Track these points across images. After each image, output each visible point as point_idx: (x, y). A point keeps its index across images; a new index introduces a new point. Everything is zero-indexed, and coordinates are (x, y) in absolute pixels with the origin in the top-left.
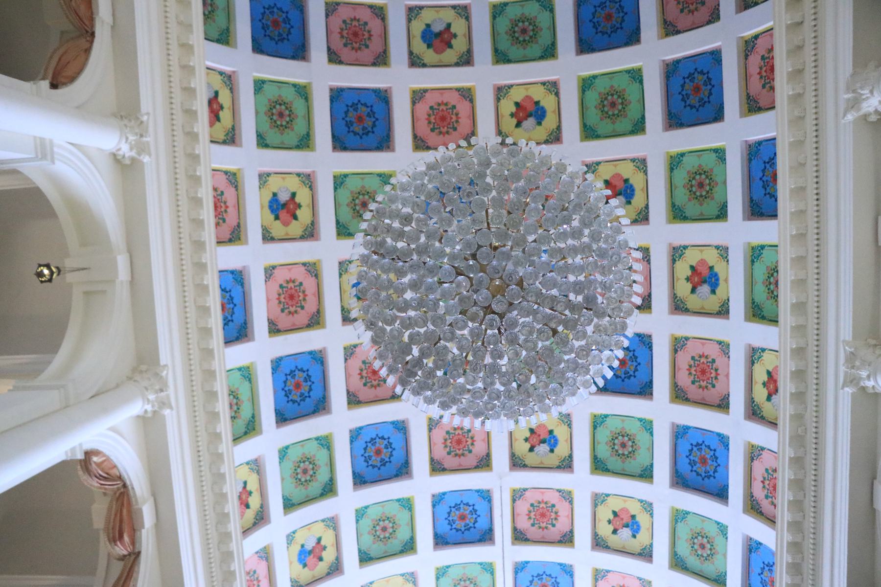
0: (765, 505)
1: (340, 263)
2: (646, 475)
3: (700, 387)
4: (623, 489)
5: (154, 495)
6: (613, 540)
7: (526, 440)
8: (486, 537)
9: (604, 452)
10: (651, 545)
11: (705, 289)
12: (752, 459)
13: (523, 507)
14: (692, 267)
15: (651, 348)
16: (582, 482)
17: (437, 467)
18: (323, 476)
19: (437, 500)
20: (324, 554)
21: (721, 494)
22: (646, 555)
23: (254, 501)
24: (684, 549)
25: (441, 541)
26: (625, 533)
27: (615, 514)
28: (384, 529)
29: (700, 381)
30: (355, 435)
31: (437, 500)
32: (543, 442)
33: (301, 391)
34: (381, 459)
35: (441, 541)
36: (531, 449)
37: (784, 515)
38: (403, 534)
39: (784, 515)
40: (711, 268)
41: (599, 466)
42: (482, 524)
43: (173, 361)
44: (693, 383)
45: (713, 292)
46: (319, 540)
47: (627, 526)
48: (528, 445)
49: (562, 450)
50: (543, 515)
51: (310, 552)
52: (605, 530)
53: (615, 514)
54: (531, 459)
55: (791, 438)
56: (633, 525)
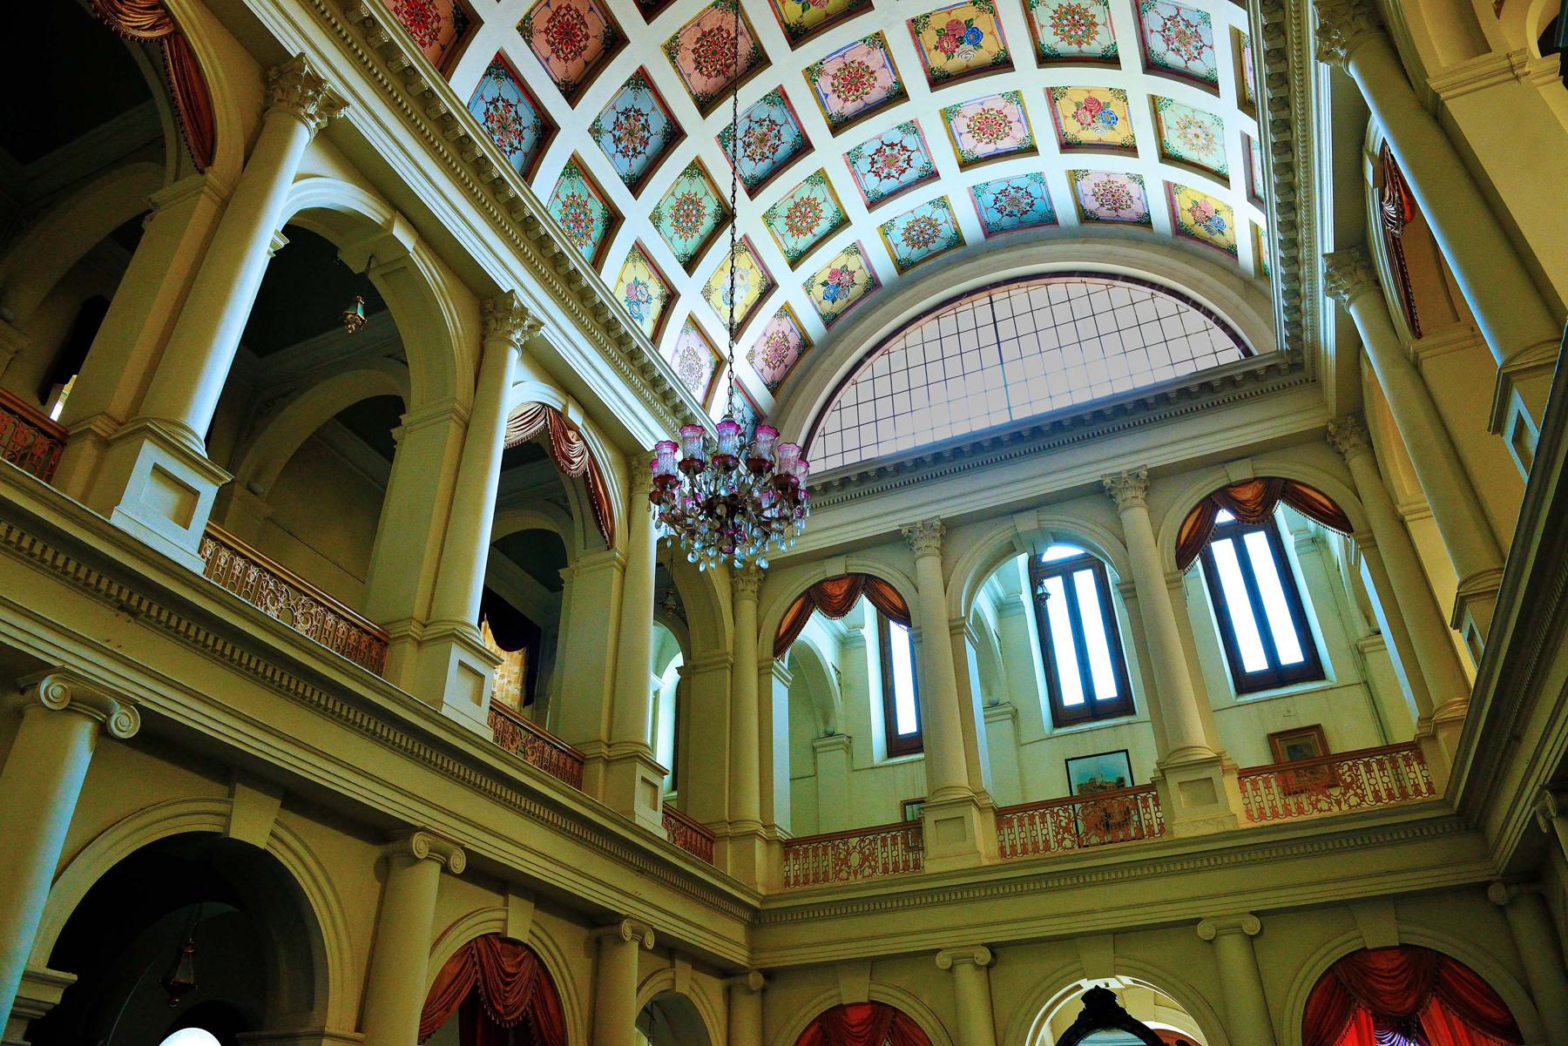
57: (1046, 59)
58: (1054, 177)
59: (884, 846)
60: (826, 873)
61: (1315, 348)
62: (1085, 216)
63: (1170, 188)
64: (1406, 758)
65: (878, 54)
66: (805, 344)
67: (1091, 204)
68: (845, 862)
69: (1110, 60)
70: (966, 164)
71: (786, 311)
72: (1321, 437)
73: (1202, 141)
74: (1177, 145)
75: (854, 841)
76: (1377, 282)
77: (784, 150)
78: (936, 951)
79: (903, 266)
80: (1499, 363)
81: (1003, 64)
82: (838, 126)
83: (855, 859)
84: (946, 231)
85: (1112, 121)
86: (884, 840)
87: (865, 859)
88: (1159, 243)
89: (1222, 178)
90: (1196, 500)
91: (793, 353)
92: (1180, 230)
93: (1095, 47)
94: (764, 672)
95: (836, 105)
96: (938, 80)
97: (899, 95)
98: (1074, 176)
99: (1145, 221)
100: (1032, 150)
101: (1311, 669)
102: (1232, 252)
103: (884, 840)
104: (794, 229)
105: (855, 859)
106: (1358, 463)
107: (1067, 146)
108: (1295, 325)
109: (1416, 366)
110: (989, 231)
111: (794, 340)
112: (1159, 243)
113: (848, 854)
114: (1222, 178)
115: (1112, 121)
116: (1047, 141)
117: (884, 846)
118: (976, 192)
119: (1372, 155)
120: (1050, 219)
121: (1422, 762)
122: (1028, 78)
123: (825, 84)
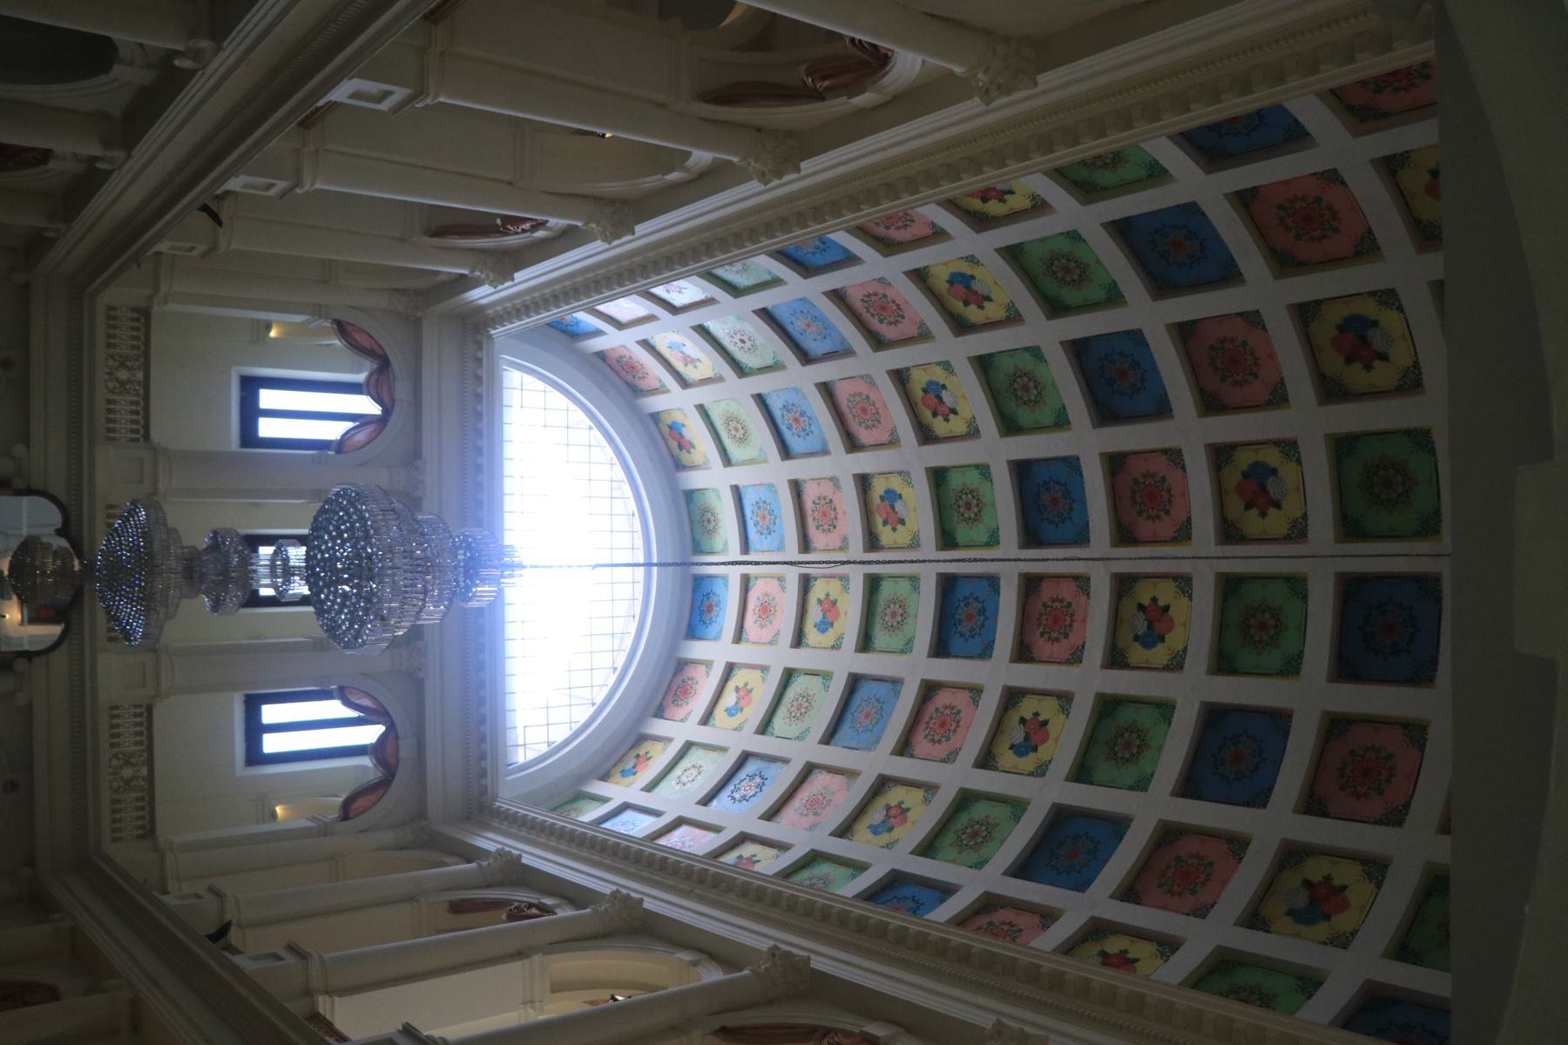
0: (983, 920)
1: (1393, 290)
2: (1081, 773)
3: (1168, 867)
4: (1066, 737)
5: (895, 98)
6: (1014, 717)
7: (1154, 600)
8: (1031, 537)
9: (1126, 715)
10: (996, 769)
11: (1302, 901)
12: (1043, 916)
13: (1067, 591)
14: (1344, 888)
15: (1247, 804)
16: (1089, 680)
17: (1115, 463)
18: (1070, 296)
19: (1072, 464)
20: (973, 307)
21: (1023, 869)
22: (986, 760)
23: (994, 207)
24: (979, 810)
25: (1022, 470)
26: (1018, 735)
27: (1045, 723)
28: (1026, 389)
29: (1177, 868)
30: (1136, 337)
31: (1072, 464)
32: (1150, 626)
33: (1172, 251)
34: (1114, 377)
35: (1022, 470)
36: (1141, 607)
37: (876, 913)
38: (1024, 416)
39: (958, 937)
40: (1328, 917)
41: (1107, 705)
42: (1145, 528)
43: (1044, 92)
44: (1178, 858)
45: (1290, 913)
46: (989, 299)
47: (1026, 739)
48: (1146, 602)
49: (1137, 653)
50: (1055, 621)
51: (968, 288)
52: (1027, 707)
53: (1045, 723)
54: (1129, 606)
55: (994, 954)
56: (1026, 747)
57: (789, 675)
59: (132, 403)
60: (114, 346)
62: (682, 665)
63: (668, 740)
64: (142, 827)
67: (690, 671)
68: (122, 365)
72: (421, 814)
73: (684, 779)
74: (695, 756)
75: (140, 376)
76: (489, 886)
78: (28, 444)
79: (689, 495)
80: (326, 956)
81: (798, 640)
83: (123, 375)
86: (137, 403)
87: (122, 384)
88: (640, 719)
89: (650, 788)
90: (389, 708)
91: (629, 378)
92: (642, 738)
93: (779, 722)
94: (318, 311)
98: (708, 664)
99: (660, 713)
100: (739, 636)
101: (255, 756)
102: (605, 777)
103: (137, 403)
104: (729, 419)
105: (123, 375)
106: (388, 837)
107: (730, 668)
109: (411, 899)
111: (643, 384)
112: (640, 719)
113: (130, 369)
114: (650, 788)
116: (739, 654)
117: (132, 403)
119: (558, 906)
121: (140, 837)
122: (783, 656)
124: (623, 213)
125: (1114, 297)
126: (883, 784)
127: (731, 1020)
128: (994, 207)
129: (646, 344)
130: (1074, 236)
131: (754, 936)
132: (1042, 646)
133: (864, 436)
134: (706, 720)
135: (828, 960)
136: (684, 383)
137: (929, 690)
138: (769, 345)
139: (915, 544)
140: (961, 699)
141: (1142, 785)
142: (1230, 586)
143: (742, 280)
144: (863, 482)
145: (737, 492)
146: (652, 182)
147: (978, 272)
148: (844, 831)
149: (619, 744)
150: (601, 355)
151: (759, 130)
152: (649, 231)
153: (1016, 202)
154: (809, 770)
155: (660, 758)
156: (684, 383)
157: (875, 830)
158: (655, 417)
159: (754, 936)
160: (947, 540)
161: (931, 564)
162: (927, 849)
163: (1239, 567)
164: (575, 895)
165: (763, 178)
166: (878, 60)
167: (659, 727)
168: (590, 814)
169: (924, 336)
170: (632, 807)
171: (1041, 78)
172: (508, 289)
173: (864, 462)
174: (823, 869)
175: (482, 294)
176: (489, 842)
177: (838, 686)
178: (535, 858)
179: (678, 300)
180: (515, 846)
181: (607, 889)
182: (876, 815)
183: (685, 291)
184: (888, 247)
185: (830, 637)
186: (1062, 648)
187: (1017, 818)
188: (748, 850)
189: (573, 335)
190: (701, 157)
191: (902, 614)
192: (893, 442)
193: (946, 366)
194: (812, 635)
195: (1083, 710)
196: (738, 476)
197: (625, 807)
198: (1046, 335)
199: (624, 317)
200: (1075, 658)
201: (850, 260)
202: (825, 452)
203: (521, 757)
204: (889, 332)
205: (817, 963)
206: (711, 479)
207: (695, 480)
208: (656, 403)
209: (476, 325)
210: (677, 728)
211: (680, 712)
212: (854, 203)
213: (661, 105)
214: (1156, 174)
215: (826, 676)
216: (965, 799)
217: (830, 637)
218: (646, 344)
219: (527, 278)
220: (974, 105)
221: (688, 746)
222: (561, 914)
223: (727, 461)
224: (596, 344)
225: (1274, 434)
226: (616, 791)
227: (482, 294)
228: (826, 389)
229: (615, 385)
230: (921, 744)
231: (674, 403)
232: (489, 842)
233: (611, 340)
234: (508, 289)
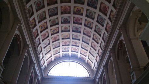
0: (108, 30)
8: (69, 23)
9: (88, 14)
24: (96, 30)
38: (57, 22)
41: (87, 16)
49: (81, 12)
57: (82, 48)
58: (79, 55)
61: (96, 80)
62: (80, 58)
65: (68, 42)
66: (52, 61)
69: (87, 51)
70: (72, 51)
71: (52, 58)
74: (89, 58)
77: (57, 46)
79: (63, 56)
81: (78, 46)
82: (63, 46)
84: (68, 55)
85: (85, 54)
88: (85, 63)
92: (87, 63)
93: (86, 49)
95: (63, 44)
96: (72, 45)
97: (69, 45)
99: (85, 61)
100: (78, 52)
107: (81, 53)
108: (95, 78)
110: (72, 56)
112: (85, 63)
114: (92, 63)
115: (85, 54)
116: (79, 52)
118: (71, 53)
120: (77, 57)
123: (63, 43)
124: (32, 62)
125: (45, 12)
126: (93, 39)
127: (117, 58)
128: (34, 24)
129: (47, 60)
130: (37, 16)
131: (108, 54)
132: (80, 30)
133: (58, 39)
134: (86, 56)
135: (111, 46)
136: (51, 56)
137: (84, 34)
138: (48, 47)
139: (69, 34)
140: (85, 30)
141: (95, 13)
142: (73, 31)
143: (40, 50)
144: (62, 39)
145: (63, 52)
146: (29, 60)
147: (41, 26)
148: (96, 50)
149: (87, 65)
150: (47, 65)
151: (23, 48)
152: (34, 60)
153: (33, 21)
154: (90, 53)
155: (90, 61)
156: (51, 56)
157: (98, 40)
158: (54, 60)
159: (108, 54)
160: (69, 31)
161: (71, 33)
162: (100, 35)
163: (72, 22)
164: (103, 72)
165: (29, 48)
166: (17, 35)
167: (86, 61)
168: (95, 69)
169: (48, 32)
170: (94, 65)
171: (19, 18)
172: (39, 75)
173: (60, 39)
174: (102, 46)
175: (39, 78)
176: (97, 80)
177: (83, 43)
178: (99, 75)
179: (42, 57)
180: (98, 77)
181: (102, 68)
182: (96, 40)
183: (41, 56)
184: (38, 35)
185: (78, 43)
186: (80, 29)
187: (95, 35)
188: (99, 53)
189: (45, 68)
190: (26, 54)
191: (76, 36)
192: (59, 35)
193: (51, 30)
194: (77, 45)
195: (87, 18)
196: (61, 51)
197: (94, 65)
198: (48, 19)
199: (43, 63)
200: (82, 19)
201: (39, 39)
202: (60, 49)
203: (88, 76)
204: (47, 35)
205: (111, 47)
206: (61, 54)
207: (61, 56)
208: (53, 59)
209: (43, 78)
210: (87, 59)
211: (85, 59)
212: (32, 38)
213: (20, 59)
214: (31, 6)
215: (82, 44)
216: (95, 31)
217: (78, 43)
218: (47, 60)
219: (38, 73)
220: (22, 25)
221: (88, 58)
222: (105, 73)
223: (60, 52)
224: (46, 65)
225: (61, 35)
226: (93, 66)
227: (39, 78)
228: (53, 49)
229: (51, 64)
230: (88, 42)
231: (53, 58)
232: (97, 80)
233: (46, 64)
234: (39, 75)
